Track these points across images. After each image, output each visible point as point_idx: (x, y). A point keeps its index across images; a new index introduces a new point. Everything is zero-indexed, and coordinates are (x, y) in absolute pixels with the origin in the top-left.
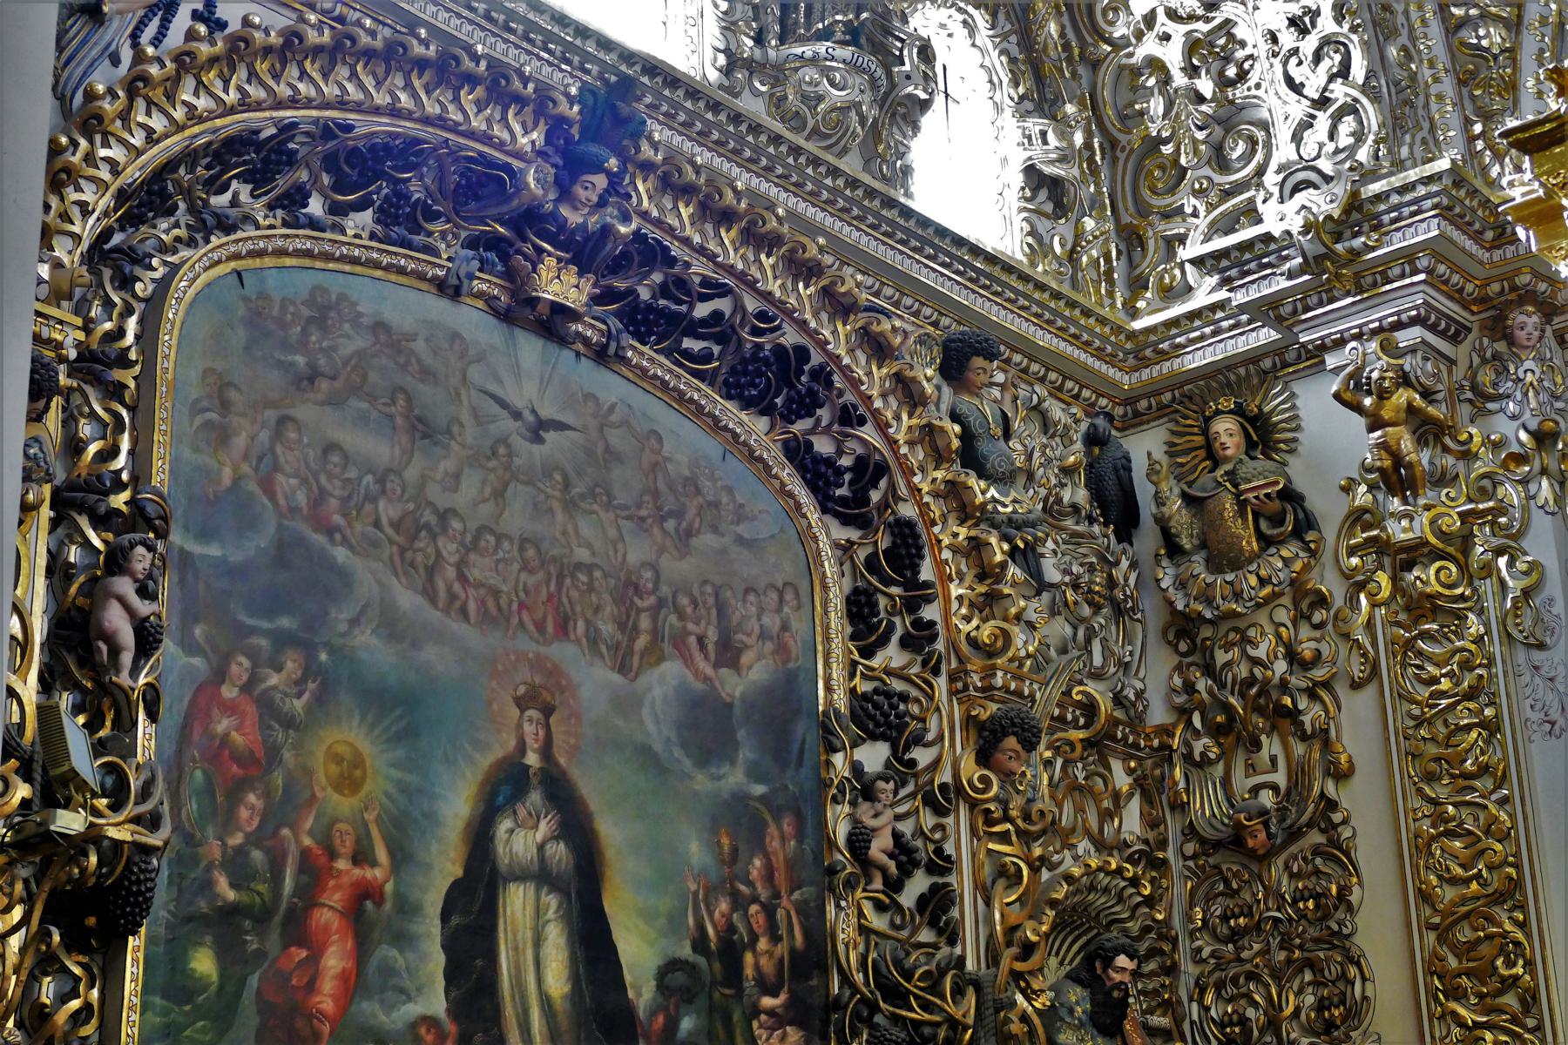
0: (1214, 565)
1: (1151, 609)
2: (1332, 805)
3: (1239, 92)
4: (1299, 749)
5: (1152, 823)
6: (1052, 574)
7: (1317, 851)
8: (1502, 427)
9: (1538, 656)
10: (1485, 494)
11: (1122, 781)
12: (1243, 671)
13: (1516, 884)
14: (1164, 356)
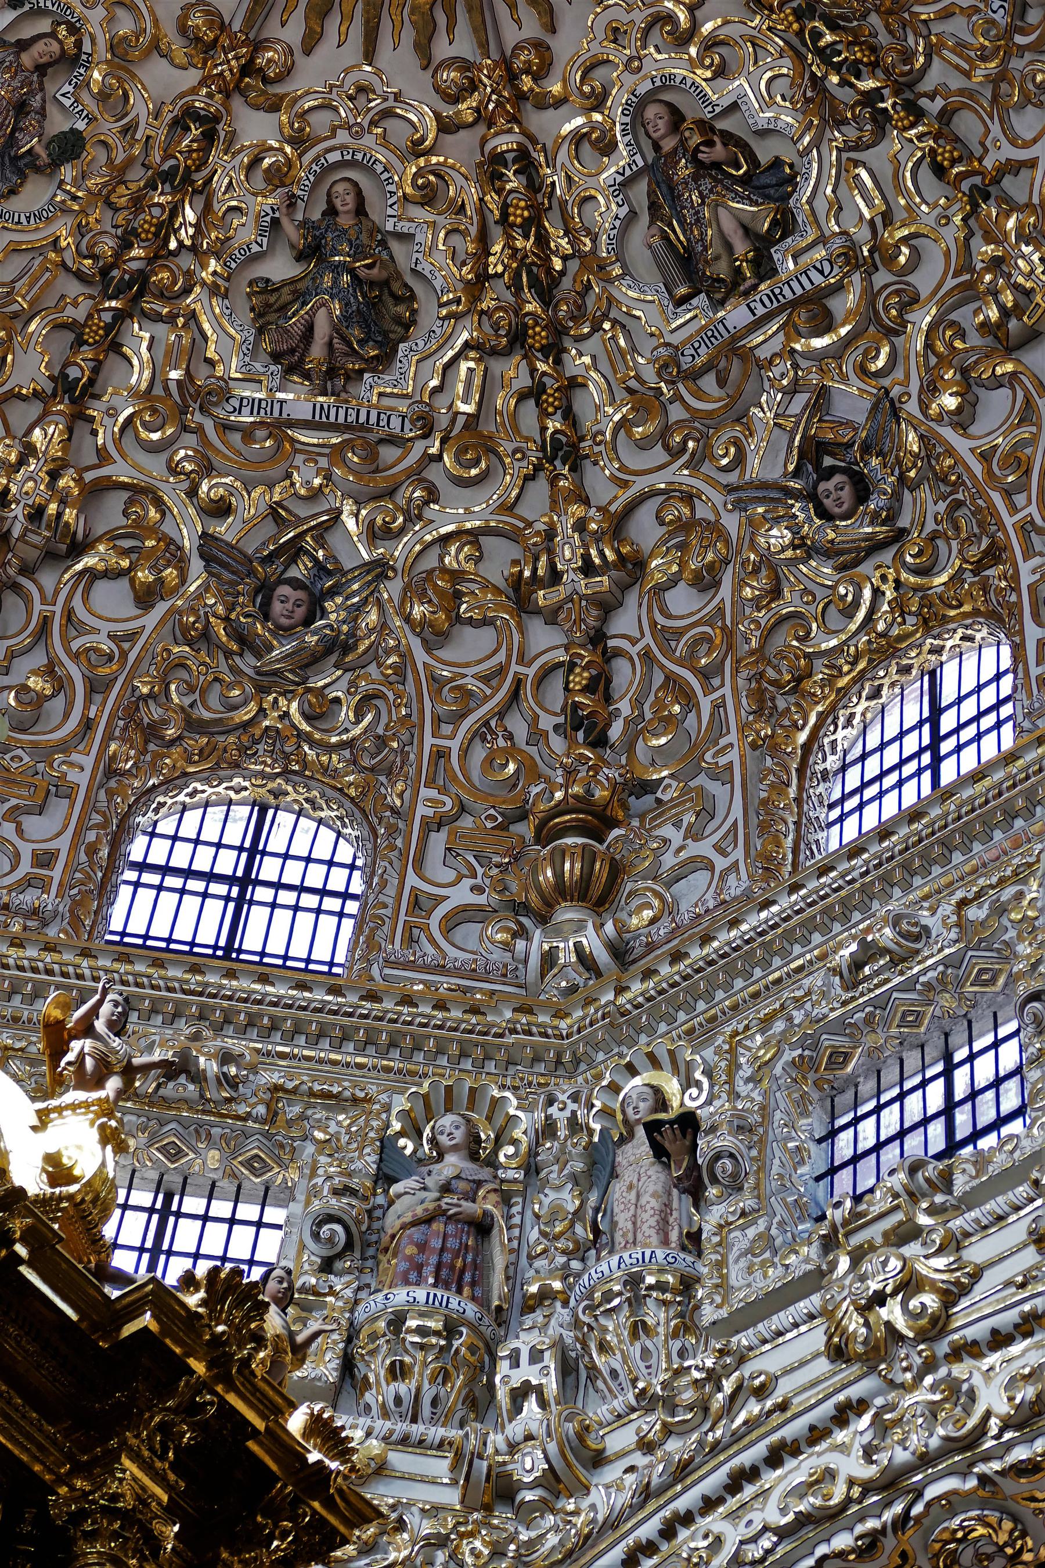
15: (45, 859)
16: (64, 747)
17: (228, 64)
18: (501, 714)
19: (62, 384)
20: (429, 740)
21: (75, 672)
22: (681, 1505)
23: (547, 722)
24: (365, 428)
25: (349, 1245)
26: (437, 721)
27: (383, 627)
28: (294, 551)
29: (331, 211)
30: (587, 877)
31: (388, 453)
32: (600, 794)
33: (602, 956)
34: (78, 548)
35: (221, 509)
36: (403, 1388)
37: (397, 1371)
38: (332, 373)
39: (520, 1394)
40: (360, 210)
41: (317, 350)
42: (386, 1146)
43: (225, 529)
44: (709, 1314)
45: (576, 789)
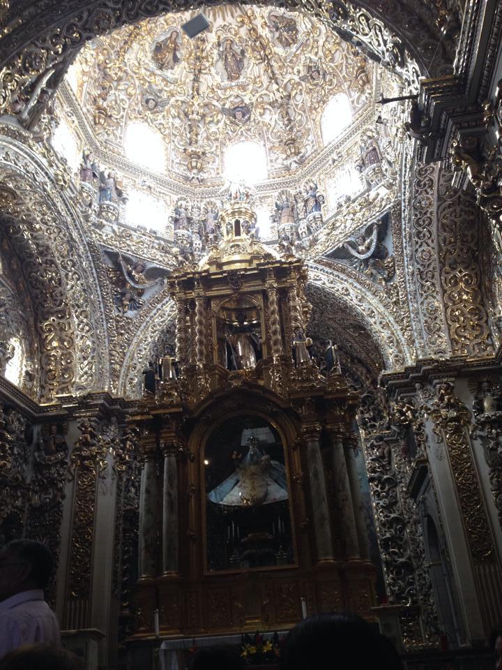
0: (47, 454)
1: (31, 459)
2: (61, 503)
3: (69, 366)
4: (56, 492)
5: (23, 503)
6: (16, 452)
7: (56, 512)
8: (105, 437)
9: (104, 480)
10: (100, 449)
11: (19, 494)
12: (48, 475)
13: (92, 522)
14: (45, 412)
15: (312, 142)
16: (306, 124)
17: (246, 20)
18: (347, 62)
19: (271, 78)
20: (341, 76)
21: (301, 112)
22: (403, 174)
23: (352, 56)
24: (302, 44)
25: (361, 167)
26: (340, 71)
27: (327, 66)
28: (310, 68)
29: (274, 22)
30: (363, 81)
31: (308, 42)
32: (359, 65)
33: (370, 91)
34: (289, 96)
35: (299, 72)
36: (374, 182)
37: (372, 181)
38: (293, 40)
39: (386, 170)
40: (276, 17)
41: (290, 40)
42: (361, 147)
43: (302, 74)
44: (392, 145)
45: (356, 68)
